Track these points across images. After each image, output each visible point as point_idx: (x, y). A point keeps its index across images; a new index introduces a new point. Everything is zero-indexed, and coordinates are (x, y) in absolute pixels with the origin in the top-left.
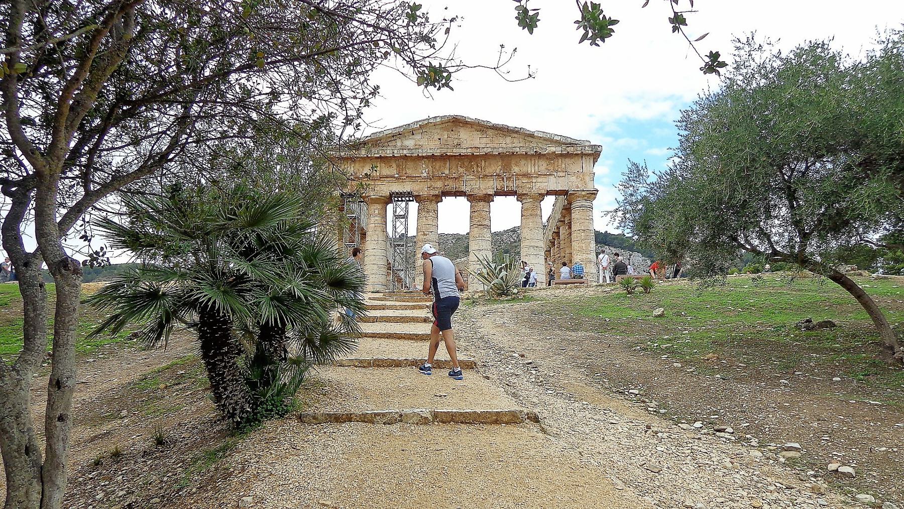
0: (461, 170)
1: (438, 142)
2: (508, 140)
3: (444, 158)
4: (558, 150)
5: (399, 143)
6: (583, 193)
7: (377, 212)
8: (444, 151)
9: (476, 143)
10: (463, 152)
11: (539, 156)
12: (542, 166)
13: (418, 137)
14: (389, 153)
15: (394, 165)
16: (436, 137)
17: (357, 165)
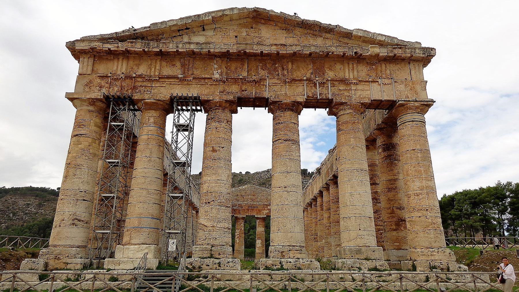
0: (263, 73)
1: (234, 40)
2: (319, 41)
3: (242, 57)
4: (383, 52)
5: (186, 39)
6: (417, 104)
7: (152, 120)
8: (242, 47)
9: (283, 42)
10: (266, 50)
11: (359, 58)
12: (362, 71)
13: (210, 33)
14: (171, 47)
15: (178, 64)
16: (232, 34)
17: (131, 62)
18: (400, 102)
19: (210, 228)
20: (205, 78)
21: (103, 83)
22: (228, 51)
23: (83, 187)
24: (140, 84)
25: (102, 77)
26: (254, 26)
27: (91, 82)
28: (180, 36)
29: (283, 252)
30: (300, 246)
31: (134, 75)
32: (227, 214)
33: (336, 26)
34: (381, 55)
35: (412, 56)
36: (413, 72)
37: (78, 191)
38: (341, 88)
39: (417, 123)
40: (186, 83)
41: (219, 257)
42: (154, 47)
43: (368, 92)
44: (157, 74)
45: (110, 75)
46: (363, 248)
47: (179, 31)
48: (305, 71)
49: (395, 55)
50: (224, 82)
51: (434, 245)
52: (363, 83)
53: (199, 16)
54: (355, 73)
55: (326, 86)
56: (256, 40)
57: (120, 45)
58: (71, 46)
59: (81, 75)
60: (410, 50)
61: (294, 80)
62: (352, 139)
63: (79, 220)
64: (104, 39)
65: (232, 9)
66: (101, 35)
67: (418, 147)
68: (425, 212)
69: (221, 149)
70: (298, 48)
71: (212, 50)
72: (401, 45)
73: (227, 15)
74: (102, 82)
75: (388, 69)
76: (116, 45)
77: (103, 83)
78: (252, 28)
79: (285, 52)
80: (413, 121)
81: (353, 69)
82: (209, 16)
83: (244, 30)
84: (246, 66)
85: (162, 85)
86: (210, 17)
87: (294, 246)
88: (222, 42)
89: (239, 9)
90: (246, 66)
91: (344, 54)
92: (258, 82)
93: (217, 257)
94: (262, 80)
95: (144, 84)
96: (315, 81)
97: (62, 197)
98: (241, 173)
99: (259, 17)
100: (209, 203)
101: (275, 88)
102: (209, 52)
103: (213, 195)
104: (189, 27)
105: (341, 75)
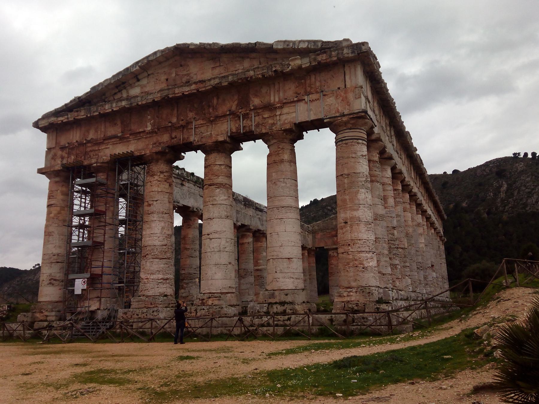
0: (191, 115)
2: (246, 64)
4: (305, 62)
6: (345, 119)
11: (282, 77)
12: (289, 90)
13: (144, 82)
14: (107, 108)
15: (119, 123)
16: (163, 78)
18: (325, 121)
19: (146, 280)
20: (140, 133)
22: (154, 100)
23: (56, 251)
24: (90, 149)
25: (63, 148)
26: (183, 63)
27: (55, 155)
28: (119, 91)
29: (203, 299)
30: (222, 293)
31: (85, 142)
32: (162, 266)
33: (256, 43)
34: (303, 66)
35: (339, 59)
36: (347, 77)
37: (52, 255)
38: (266, 116)
39: (347, 141)
40: (125, 140)
41: (151, 306)
43: (294, 115)
44: (102, 136)
45: (67, 145)
46: (277, 293)
47: (117, 87)
48: (231, 104)
49: (319, 63)
50: (156, 133)
51: (353, 284)
52: (289, 105)
53: (127, 69)
54: (281, 94)
55: (250, 116)
56: (184, 80)
57: (69, 116)
58: (36, 125)
59: (49, 149)
60: (337, 52)
61: (218, 118)
62: (274, 174)
63: (55, 280)
64: (57, 113)
65: (155, 53)
66: (56, 110)
67: (346, 172)
69: (155, 203)
70: (217, 81)
71: (140, 103)
72: (326, 47)
73: (152, 61)
75: (316, 81)
76: (66, 117)
78: (181, 66)
79: (203, 89)
80: (342, 141)
81: (279, 91)
82: (136, 67)
83: (174, 71)
84: (175, 111)
86: (137, 68)
87: (214, 293)
88: (152, 88)
89: (162, 51)
90: (175, 111)
91: (263, 76)
93: (150, 306)
94: (189, 123)
96: (238, 113)
98: (445, 173)
99: (182, 54)
101: (202, 129)
102: (138, 104)
104: (124, 81)
105: (266, 100)
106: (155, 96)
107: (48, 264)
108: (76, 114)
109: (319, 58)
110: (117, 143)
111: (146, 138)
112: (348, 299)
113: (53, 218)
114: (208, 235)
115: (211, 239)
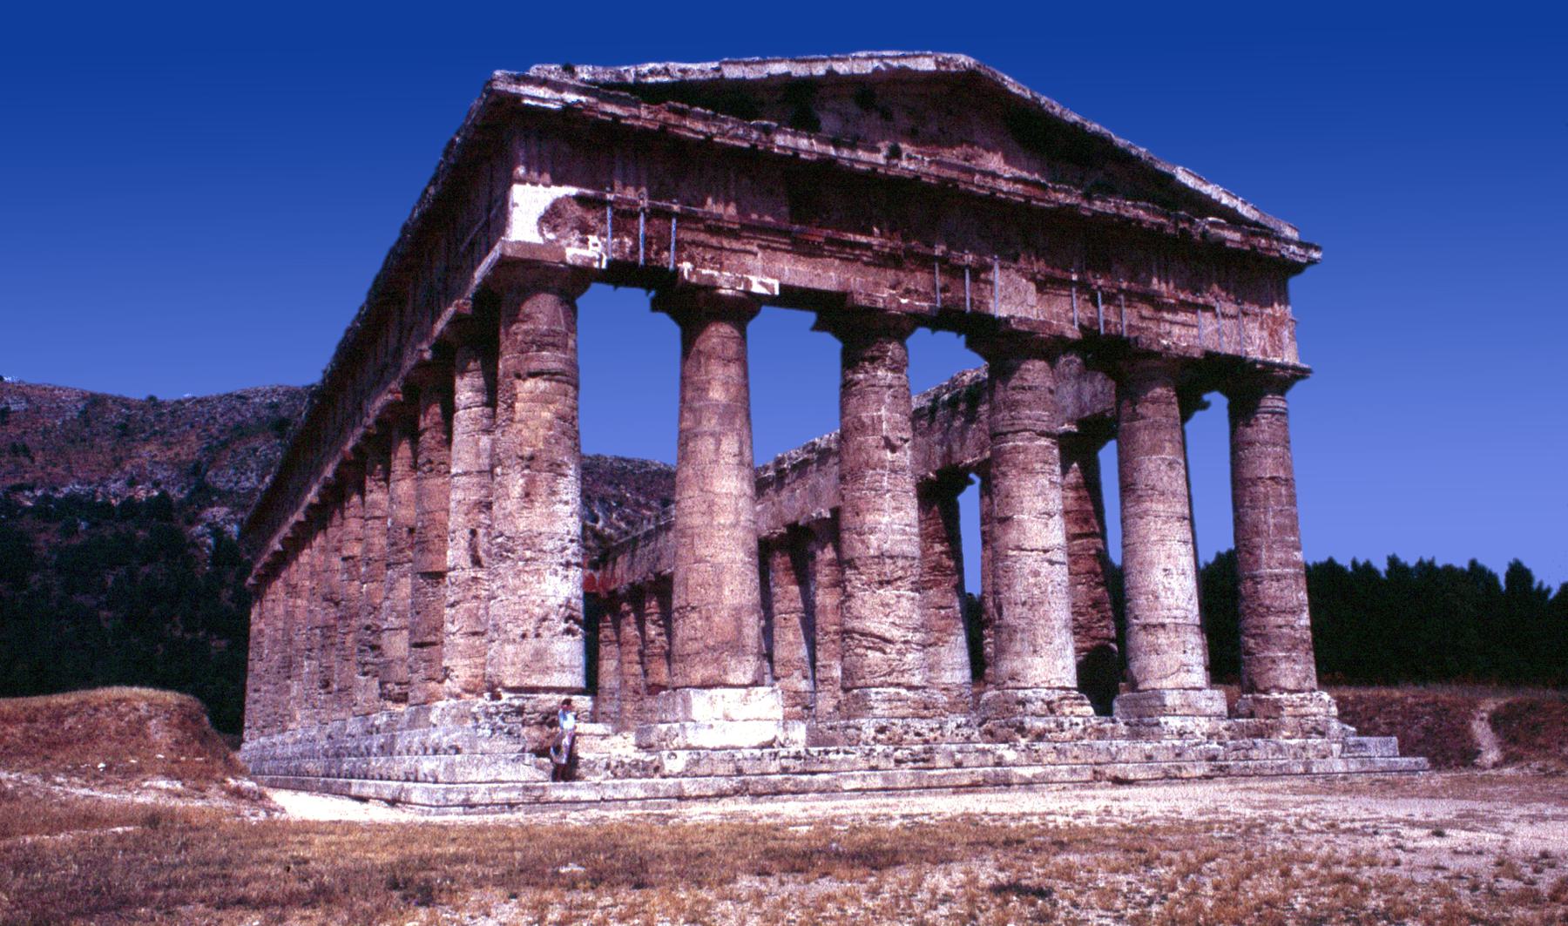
21: (591, 219)
42: (732, 133)
45: (610, 197)
62: (1168, 445)
68: (1290, 618)
71: (881, 170)
74: (589, 217)
76: (634, 111)
77: (591, 219)
85: (748, 247)
92: (979, 273)
95: (702, 237)
97: (528, 554)
100: (889, 582)
103: (900, 563)
106: (924, 170)
107: (560, 569)
108: (673, 119)
109: (1255, 241)
110: (775, 249)
111: (867, 264)
112: (1303, 711)
113: (562, 418)
114: (1045, 551)
115: (1052, 563)
